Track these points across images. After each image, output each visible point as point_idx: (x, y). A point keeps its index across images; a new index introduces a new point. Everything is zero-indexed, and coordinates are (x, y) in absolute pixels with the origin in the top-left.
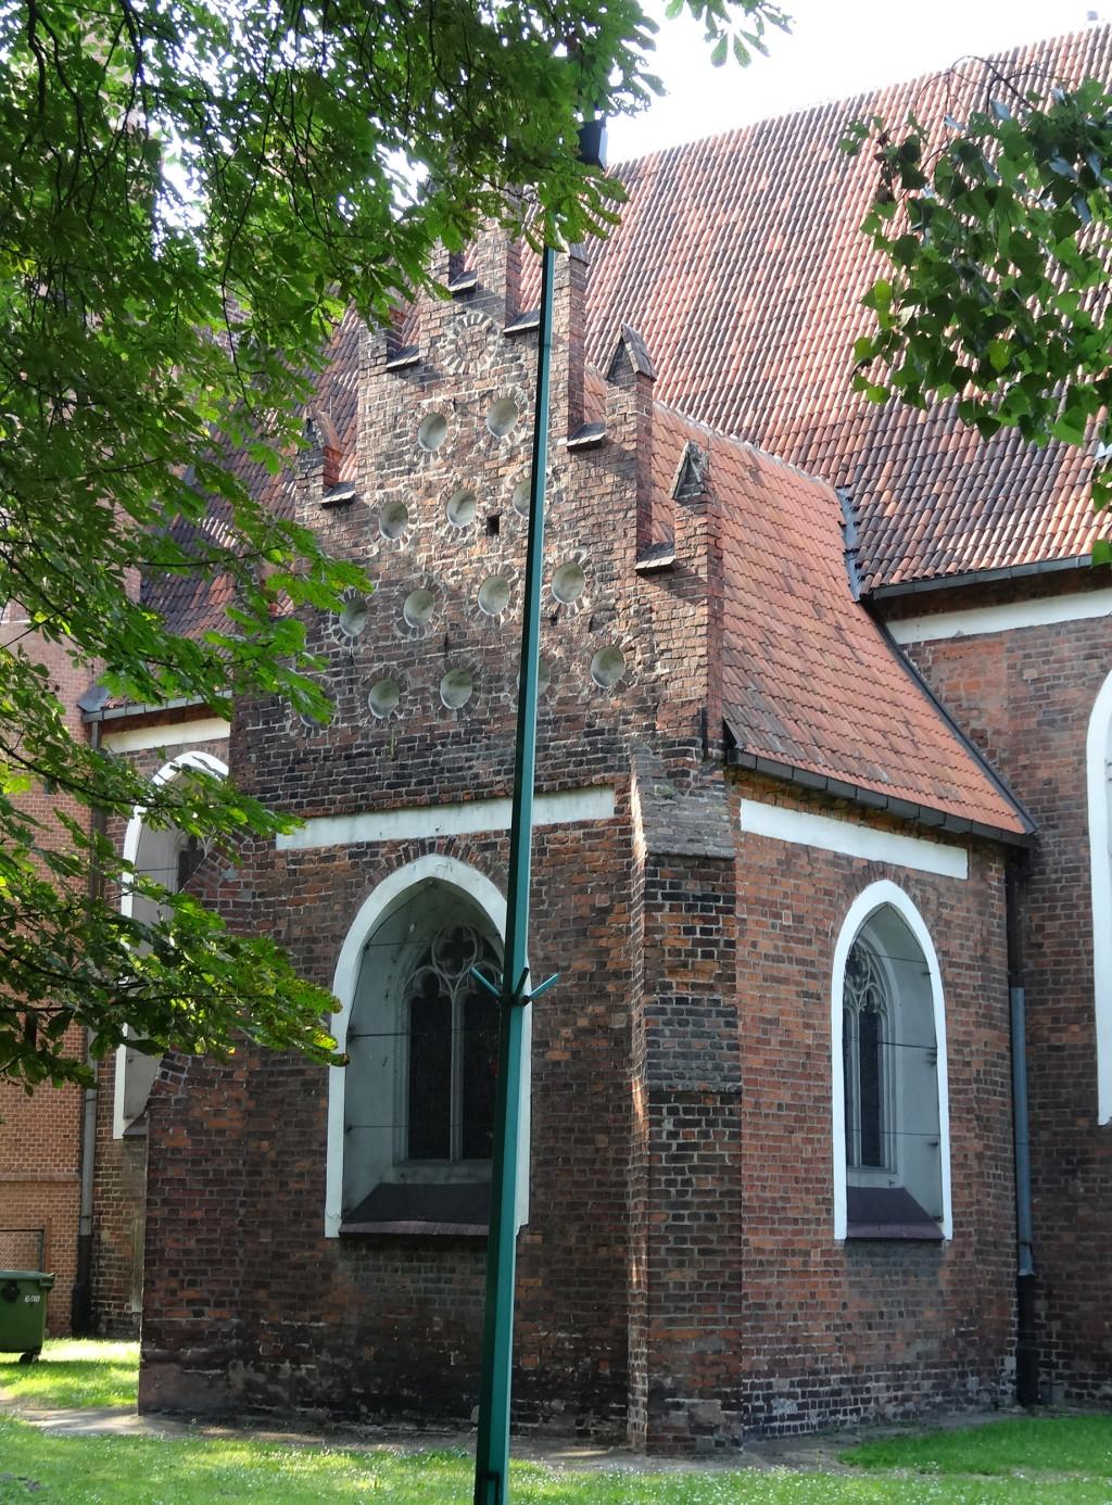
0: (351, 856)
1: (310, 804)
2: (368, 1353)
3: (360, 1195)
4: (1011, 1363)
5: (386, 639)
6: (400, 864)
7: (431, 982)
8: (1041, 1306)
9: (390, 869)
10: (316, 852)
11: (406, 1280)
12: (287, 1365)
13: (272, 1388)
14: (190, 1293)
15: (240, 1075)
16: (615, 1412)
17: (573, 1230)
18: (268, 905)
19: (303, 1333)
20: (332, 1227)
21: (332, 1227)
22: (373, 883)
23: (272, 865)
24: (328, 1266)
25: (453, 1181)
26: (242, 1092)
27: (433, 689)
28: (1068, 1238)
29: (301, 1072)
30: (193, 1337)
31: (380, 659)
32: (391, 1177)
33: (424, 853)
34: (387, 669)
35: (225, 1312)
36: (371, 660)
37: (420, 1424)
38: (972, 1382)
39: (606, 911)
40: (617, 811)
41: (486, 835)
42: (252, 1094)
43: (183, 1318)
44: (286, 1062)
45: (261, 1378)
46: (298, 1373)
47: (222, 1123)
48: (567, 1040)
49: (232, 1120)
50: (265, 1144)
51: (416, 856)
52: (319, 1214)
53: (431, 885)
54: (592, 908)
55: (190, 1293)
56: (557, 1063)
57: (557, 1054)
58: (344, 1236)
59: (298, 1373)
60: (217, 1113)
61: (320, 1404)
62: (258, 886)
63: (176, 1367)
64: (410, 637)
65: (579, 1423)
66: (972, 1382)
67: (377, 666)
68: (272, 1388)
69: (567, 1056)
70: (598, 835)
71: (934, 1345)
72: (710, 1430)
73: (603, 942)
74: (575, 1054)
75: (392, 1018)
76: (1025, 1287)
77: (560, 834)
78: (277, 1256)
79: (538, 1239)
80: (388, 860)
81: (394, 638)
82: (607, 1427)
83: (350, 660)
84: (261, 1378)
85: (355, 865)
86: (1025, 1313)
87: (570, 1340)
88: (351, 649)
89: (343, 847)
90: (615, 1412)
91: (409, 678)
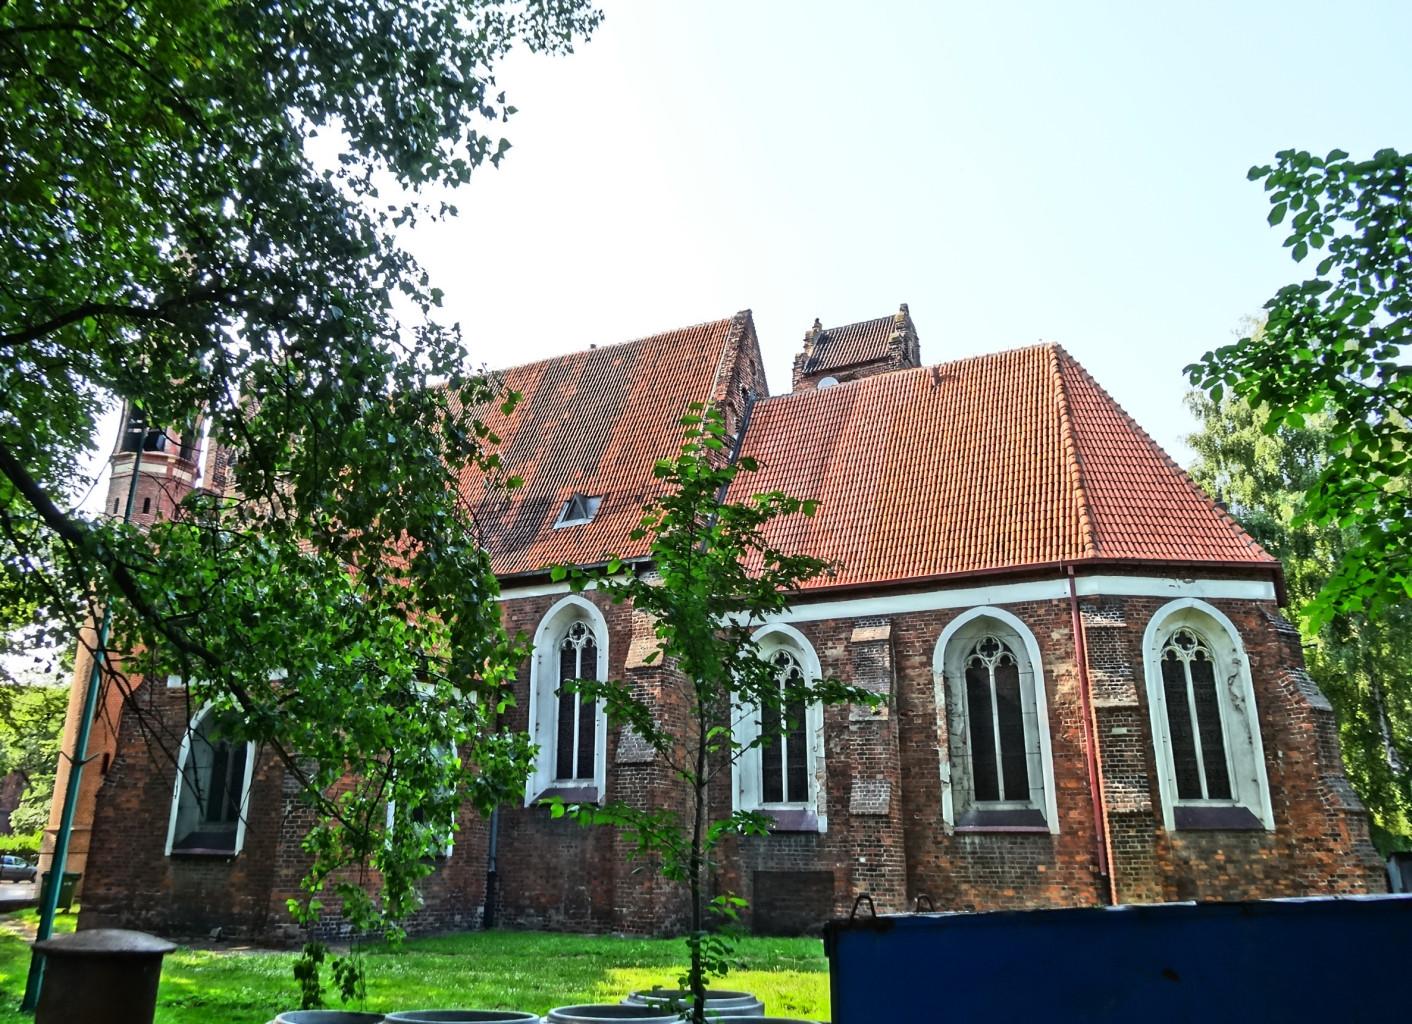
2: (176, 906)
3: (182, 837)
4: (481, 909)
8: (497, 884)
11: (195, 875)
14: (106, 881)
15: (141, 784)
17: (259, 853)
19: (151, 898)
20: (168, 851)
21: (168, 851)
24: (165, 868)
26: (141, 792)
28: (509, 855)
30: (105, 900)
32: (197, 829)
35: (121, 889)
37: (192, 937)
38: (458, 918)
42: (145, 793)
43: (101, 891)
47: (129, 805)
49: (134, 804)
52: (164, 846)
55: (106, 881)
57: (261, 777)
58: (173, 855)
60: (128, 801)
63: (95, 914)
66: (458, 918)
71: (438, 901)
72: (294, 937)
75: (205, 761)
76: (491, 877)
78: (146, 864)
86: (490, 888)
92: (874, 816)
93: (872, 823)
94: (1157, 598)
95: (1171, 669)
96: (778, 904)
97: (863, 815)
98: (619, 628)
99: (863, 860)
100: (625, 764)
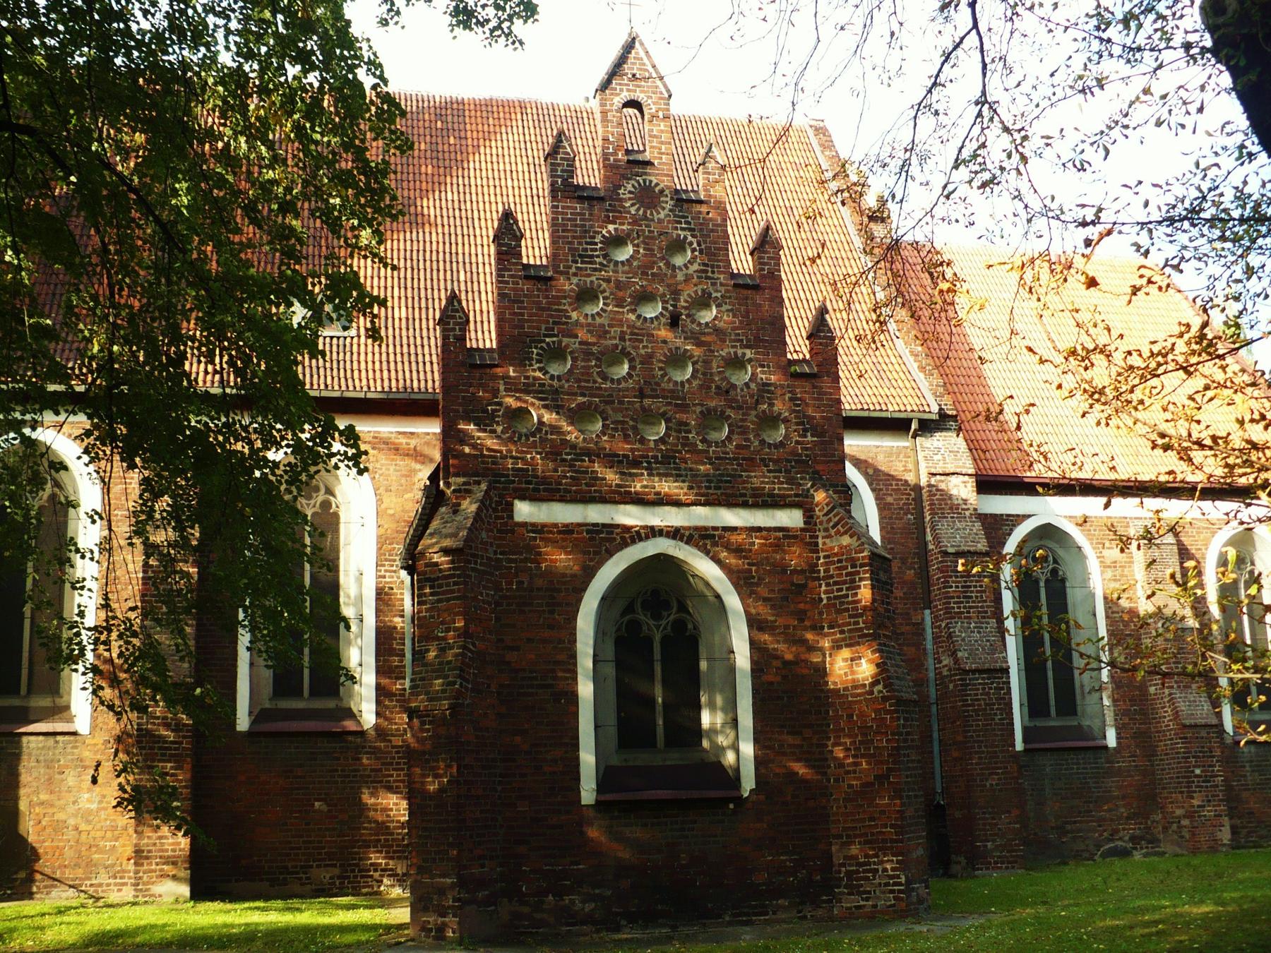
0: (588, 532)
1: (545, 490)
5: (588, 381)
6: (633, 542)
7: (634, 626)
9: (624, 544)
10: (555, 525)
12: (551, 897)
13: (538, 916)
16: (825, 901)
18: (511, 561)
22: (610, 554)
23: (513, 532)
25: (668, 763)
27: (631, 423)
29: (551, 686)
31: (583, 395)
33: (654, 536)
34: (590, 403)
36: (575, 394)
37: (674, 928)
39: (804, 586)
40: (805, 523)
41: (706, 529)
44: (535, 679)
45: (526, 910)
46: (561, 903)
48: (778, 668)
50: (518, 739)
51: (647, 538)
53: (662, 560)
54: (793, 584)
56: (772, 683)
57: (770, 677)
58: (599, 804)
59: (561, 903)
61: (583, 923)
62: (499, 546)
64: (609, 385)
65: (799, 912)
67: (580, 399)
68: (538, 916)
69: (779, 679)
70: (795, 537)
73: (802, 606)
74: (784, 677)
77: (764, 533)
79: (762, 797)
80: (623, 538)
81: (595, 382)
82: (820, 912)
83: (556, 392)
84: (526, 910)
85: (592, 539)
87: (791, 861)
88: (555, 383)
89: (579, 525)
90: (825, 901)
91: (610, 412)
92: (1206, 726)
93: (1203, 733)
94: (1018, 516)
95: (1026, 587)
96: (1068, 827)
97: (1196, 726)
98: (890, 499)
99: (1198, 771)
100: (974, 672)
